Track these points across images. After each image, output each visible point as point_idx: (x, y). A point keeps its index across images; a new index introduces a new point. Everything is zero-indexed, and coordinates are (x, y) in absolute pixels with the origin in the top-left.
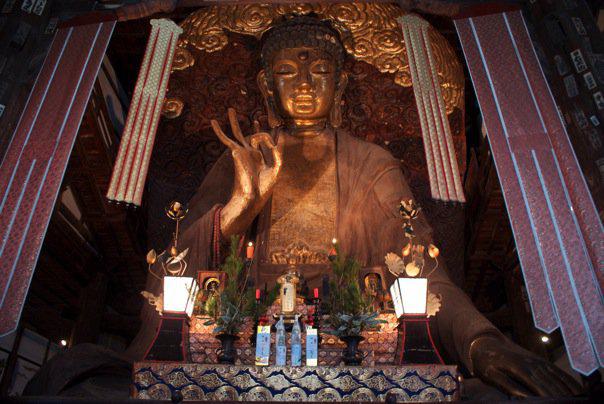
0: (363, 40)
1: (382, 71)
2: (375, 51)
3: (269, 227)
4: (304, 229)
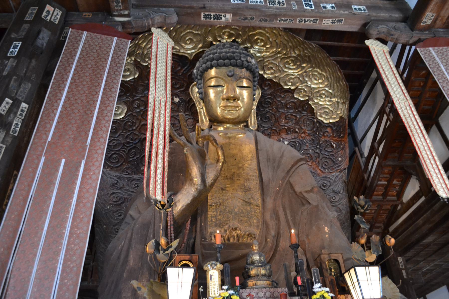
0: (272, 63)
1: (285, 87)
2: (282, 71)
3: (207, 211)
4: (236, 214)
